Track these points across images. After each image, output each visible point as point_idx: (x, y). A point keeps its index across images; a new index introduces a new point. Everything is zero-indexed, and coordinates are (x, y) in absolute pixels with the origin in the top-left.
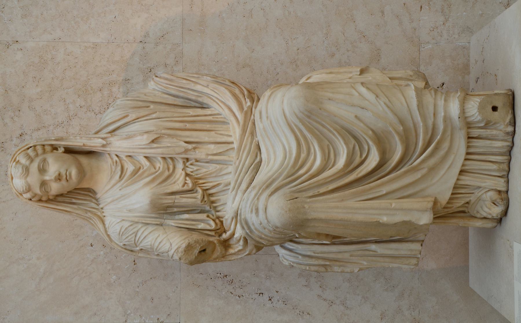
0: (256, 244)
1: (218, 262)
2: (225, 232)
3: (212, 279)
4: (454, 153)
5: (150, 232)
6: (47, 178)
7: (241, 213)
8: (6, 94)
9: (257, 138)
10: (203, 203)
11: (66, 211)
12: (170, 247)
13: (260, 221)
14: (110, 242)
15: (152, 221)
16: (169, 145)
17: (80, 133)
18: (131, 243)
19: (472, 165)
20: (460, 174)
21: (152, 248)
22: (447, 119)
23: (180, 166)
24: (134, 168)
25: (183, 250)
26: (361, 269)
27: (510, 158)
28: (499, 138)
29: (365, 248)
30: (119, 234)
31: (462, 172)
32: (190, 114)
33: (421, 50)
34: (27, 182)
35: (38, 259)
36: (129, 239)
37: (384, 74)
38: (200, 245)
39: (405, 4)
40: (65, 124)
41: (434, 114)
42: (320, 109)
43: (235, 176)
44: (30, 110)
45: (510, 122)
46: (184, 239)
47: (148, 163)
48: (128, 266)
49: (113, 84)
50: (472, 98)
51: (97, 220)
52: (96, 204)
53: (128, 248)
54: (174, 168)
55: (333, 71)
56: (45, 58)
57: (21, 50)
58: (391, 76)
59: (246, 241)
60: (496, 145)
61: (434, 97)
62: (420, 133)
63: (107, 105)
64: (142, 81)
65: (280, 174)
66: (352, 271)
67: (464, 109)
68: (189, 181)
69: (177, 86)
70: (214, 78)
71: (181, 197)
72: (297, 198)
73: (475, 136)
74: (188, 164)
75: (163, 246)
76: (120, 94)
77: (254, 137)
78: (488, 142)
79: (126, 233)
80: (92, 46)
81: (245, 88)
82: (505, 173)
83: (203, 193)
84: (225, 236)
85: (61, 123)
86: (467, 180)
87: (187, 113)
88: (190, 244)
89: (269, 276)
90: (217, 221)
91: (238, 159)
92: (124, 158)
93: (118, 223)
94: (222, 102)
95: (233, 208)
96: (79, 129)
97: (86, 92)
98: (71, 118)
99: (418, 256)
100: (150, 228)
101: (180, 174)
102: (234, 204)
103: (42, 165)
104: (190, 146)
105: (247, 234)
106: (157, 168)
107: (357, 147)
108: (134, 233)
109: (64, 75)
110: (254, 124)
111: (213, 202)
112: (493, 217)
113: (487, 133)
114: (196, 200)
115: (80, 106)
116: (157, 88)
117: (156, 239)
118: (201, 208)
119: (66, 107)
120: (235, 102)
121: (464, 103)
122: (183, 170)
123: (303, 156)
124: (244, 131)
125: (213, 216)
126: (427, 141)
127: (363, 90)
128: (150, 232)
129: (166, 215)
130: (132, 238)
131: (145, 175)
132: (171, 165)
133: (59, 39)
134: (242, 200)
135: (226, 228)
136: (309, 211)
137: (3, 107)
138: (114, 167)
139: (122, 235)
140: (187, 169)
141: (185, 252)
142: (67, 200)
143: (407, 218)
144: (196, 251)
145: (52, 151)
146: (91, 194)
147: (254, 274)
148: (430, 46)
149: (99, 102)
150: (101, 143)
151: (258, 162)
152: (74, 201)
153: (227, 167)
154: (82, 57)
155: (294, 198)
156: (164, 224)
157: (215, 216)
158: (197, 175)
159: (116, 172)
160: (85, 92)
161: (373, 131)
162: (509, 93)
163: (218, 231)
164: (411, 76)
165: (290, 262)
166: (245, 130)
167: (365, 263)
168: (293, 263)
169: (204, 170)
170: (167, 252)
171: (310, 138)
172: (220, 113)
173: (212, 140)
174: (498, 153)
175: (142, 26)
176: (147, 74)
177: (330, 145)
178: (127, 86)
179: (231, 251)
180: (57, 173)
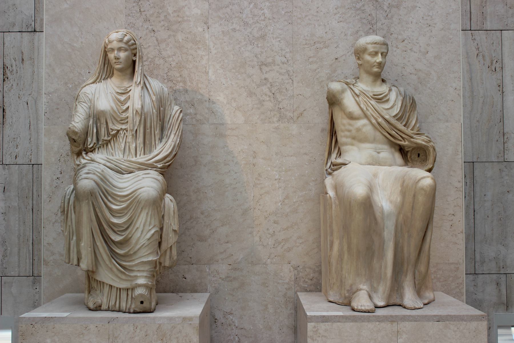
2: (86, 154)
6: (116, 52)
16: (135, 121)
19: (114, 291)
20: (110, 285)
22: (136, 277)
23: (124, 127)
24: (122, 100)
25: (74, 130)
30: (85, 93)
31: (111, 286)
32: (155, 132)
34: (113, 41)
35: (82, 42)
37: (174, 243)
39: (232, 255)
42: (142, 208)
45: (135, 311)
46: (80, 130)
51: (93, 80)
52: (105, 78)
54: (123, 124)
55: (176, 215)
56: (199, 44)
57: (204, 31)
58: (173, 247)
59: (78, 165)
61: (148, 270)
67: (141, 286)
68: (114, 132)
69: (174, 122)
71: (105, 128)
74: (125, 131)
80: (207, 71)
81: (172, 162)
84: (84, 153)
86: (106, 289)
89: (71, 177)
90: (93, 149)
92: (128, 94)
94: (163, 150)
95: (96, 158)
100: (87, 110)
101: (119, 127)
104: (134, 132)
106: (122, 114)
110: (146, 169)
111: (103, 146)
117: (81, 114)
120: (161, 158)
121: (144, 286)
122: (121, 128)
123: (119, 199)
125: (96, 146)
131: (118, 107)
138: (123, 88)
140: (122, 131)
144: (74, 137)
145: (132, 53)
146: (111, 75)
148: (207, 270)
150: (137, 81)
151: (122, 172)
152: (106, 66)
153: (122, 154)
157: (95, 147)
158: (118, 137)
161: (131, 237)
162: (151, 309)
164: (173, 258)
166: (142, 165)
167: (66, 234)
168: (66, 193)
169: (121, 141)
178: (183, 91)
179: (75, 157)
180: (119, 57)
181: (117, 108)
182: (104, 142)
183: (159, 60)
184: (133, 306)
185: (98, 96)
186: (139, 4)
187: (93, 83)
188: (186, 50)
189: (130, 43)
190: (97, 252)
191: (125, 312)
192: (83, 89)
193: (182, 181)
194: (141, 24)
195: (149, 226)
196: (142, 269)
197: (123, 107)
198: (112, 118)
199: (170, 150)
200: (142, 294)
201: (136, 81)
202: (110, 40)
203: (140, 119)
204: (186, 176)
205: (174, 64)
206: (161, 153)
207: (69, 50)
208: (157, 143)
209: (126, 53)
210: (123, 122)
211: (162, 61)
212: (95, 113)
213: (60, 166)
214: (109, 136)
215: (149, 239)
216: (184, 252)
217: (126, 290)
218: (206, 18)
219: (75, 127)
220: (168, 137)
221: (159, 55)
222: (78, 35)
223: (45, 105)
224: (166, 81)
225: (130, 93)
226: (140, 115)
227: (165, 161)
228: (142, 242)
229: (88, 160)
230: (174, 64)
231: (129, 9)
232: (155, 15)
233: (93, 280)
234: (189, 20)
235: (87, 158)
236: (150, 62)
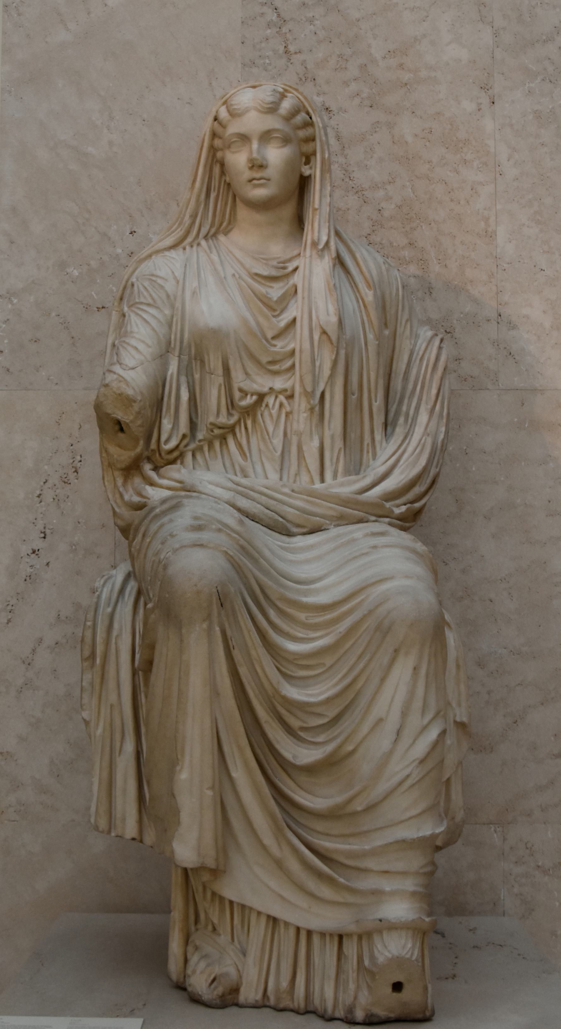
0: (133, 526)
1: (101, 457)
2: (156, 469)
3: (72, 445)
5: (153, 329)
7: (191, 497)
9: (332, 526)
10: (208, 426)
11: (194, 181)
13: (176, 535)
14: (138, 260)
15: (176, 334)
16: (317, 364)
18: (137, 296)
20: (269, 917)
21: (126, 334)
23: (279, 383)
24: (275, 299)
26: (87, 723)
27: (302, 1012)
28: (341, 994)
29: (126, 732)
31: (274, 921)
33: (491, 826)
38: (132, 422)
40: (349, 183)
41: (386, 872)
44: (373, 124)
45: (372, 1015)
47: (282, 324)
48: (95, 297)
50: (418, 944)
53: (128, 291)
54: (276, 373)
57: (479, 110)
59: (140, 507)
60: (326, 987)
62: (349, 844)
63: (385, 255)
65: (266, 573)
66: (84, 707)
67: (396, 929)
68: (249, 400)
69: (424, 377)
70: (442, 446)
71: (220, 385)
72: (222, 606)
73: (345, 950)
74: (282, 398)
75: (130, 354)
78: (332, 972)
79: (154, 287)
82: (272, 1002)
84: (147, 468)
85: (350, 177)
87: (376, 397)
88: (133, 404)
89: (76, 549)
90: (176, 454)
91: (293, 491)
92: (291, 282)
93: (173, 272)
94: (398, 461)
95: (201, 483)
98: (360, 193)
99: (113, 830)
102: (207, 484)
105: (153, 509)
106: (274, 342)
109: (436, 182)
110: (361, 521)
111: (211, 445)
112: (189, 976)
113: (351, 972)
114: (216, 413)
115: (381, 209)
116: (419, 342)
118: (199, 423)
119: (380, 186)
120: (400, 485)
122: (271, 389)
123: (302, 616)
124: (345, 502)
125: (186, 446)
126: (335, 856)
127: (433, 734)
128: (153, 329)
130: (145, 297)
131: (262, 320)
132: (280, 366)
133: (501, 173)
134: (216, 500)
135: (162, 471)
136: (197, 629)
137: (378, 79)
138: (275, 263)
139: (151, 279)
141: (119, 394)
142: (215, 182)
143: (185, 816)
144: (120, 415)
145: (302, 154)
146: (225, 224)
147: (79, 522)
149: (390, 241)
150: (319, 239)
152: (213, 195)
154: (469, 212)
155: (222, 600)
156: (171, 356)
157: (185, 449)
158: (262, 415)
160: (406, 217)
163: (157, 455)
165: (99, 590)
168: (99, 597)
169: (271, 428)
170: (118, 361)
171: (338, 631)
172: (377, 457)
174: (312, 990)
175: (528, 318)
176: (442, 326)
177: (324, 669)
179: (120, 481)
181: (258, 324)
183: (346, 198)
184: (364, 998)
185: (195, 284)
186: (284, 30)
187: (173, 247)
190: (230, 801)
191: (332, 1019)
192: (143, 265)
196: (399, 866)
198: (243, 353)
199: (423, 462)
201: (316, 238)
202: (235, 107)
203: (334, 357)
205: (389, 209)
206: (397, 471)
210: (276, 367)
212: (185, 341)
213: (42, 516)
217: (336, 939)
218: (486, 74)
219: (127, 383)
220: (410, 421)
225: (297, 279)
226: (335, 344)
227: (410, 495)
229: (169, 488)
230: (389, 209)
233: (209, 894)
234: (435, 77)
235: (165, 482)
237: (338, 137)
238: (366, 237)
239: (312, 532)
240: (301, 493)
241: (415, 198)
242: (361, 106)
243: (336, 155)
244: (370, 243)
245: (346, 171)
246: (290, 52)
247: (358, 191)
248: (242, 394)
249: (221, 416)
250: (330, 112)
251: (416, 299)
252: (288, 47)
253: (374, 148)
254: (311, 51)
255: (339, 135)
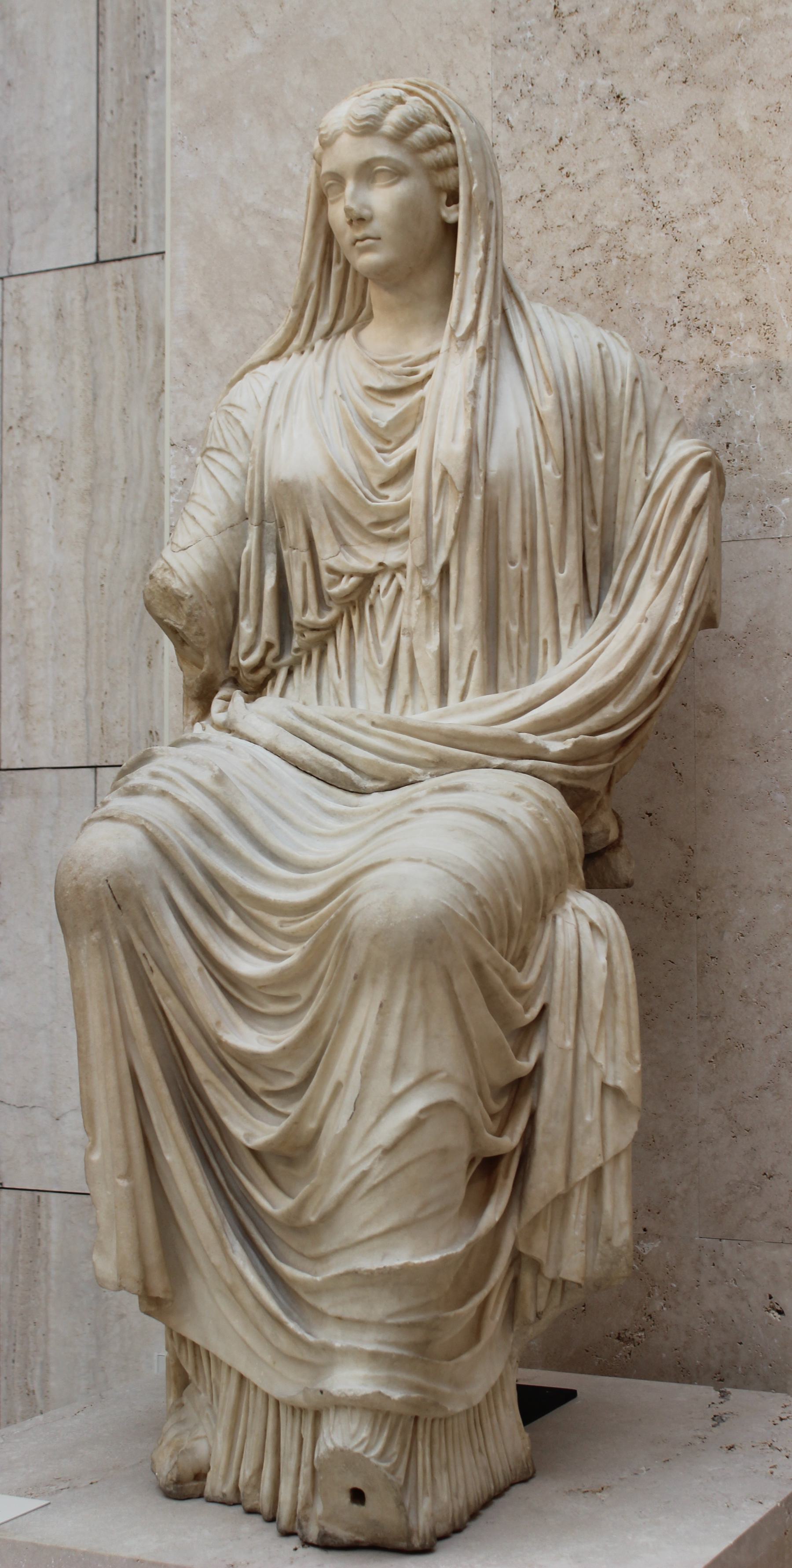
4: (274, 1363)
8: (731, 38)
9: (429, 777)
12: (179, 547)
15: (252, 492)
16: (436, 520)
17: (628, 257)
23: (392, 556)
24: (383, 424)
30: (230, 405)
34: (336, 135)
36: (215, 433)
37: (617, 1157)
40: (651, 212)
43: (330, 718)
44: (688, 110)
46: (194, 585)
49: (767, 336)
54: (390, 540)
61: (390, 1321)
63: (708, 324)
64: (777, 418)
67: (346, 1407)
68: (346, 584)
71: (304, 566)
76: (739, 356)
77: (434, 768)
79: (229, 422)
83: (322, 627)
85: (653, 202)
88: (182, 602)
90: (263, 672)
91: (373, 724)
92: (419, 394)
93: (256, 398)
96: (638, 253)
97: (743, 260)
98: (668, 227)
103: (385, 167)
106: (384, 492)
107: (289, 1083)
108: (226, 444)
117: (205, 507)
119: (699, 210)
120: (566, 706)
121: (365, 1409)
122: (381, 564)
123: (274, 921)
124: (453, 739)
125: (277, 659)
126: (296, 1288)
128: (222, 488)
129: (275, 528)
130: (216, 439)
136: (85, 942)
137: (695, 35)
138: (398, 367)
141: (164, 589)
145: (439, 190)
149: (715, 299)
151: (353, 784)
155: (119, 899)
159: (381, 377)
160: (741, 256)
164: (609, 1240)
166: (457, 742)
173: (453, 644)
178: (760, 375)
180: (365, 213)
181: (359, 467)
182: (306, 635)
183: (648, 237)
187: (275, 356)
188: (773, 167)
189: (418, 136)
193: (762, 824)
194: (561, 75)
195: (395, 1075)
196: (355, 1311)
197: (385, 460)
198: (336, 514)
199: (621, 667)
200: (349, 1451)
204: (780, 797)
205: (714, 245)
207: (265, 241)
208: (565, 629)
209: (401, 189)
210: (387, 531)
211: (658, 239)
214: (331, 604)
215: (389, 1151)
216: (770, 1177)
220: (623, 599)
221: (643, 214)
222: (296, 170)
223: (171, 493)
224: (678, 333)
227: (593, 721)
228: (353, 1167)
230: (714, 245)
231: (510, 14)
232: (626, 19)
236: (606, 249)
237: (636, 140)
238: (678, 298)
239: (395, 786)
240: (383, 727)
241: (755, 223)
242: (669, 84)
243: (632, 169)
244: (686, 307)
245: (647, 193)
246: (562, 13)
247: (666, 223)
248: (332, 576)
249: (309, 611)
250: (623, 101)
251: (756, 390)
252: (559, 7)
253: (690, 150)
254: (593, 6)
255: (636, 136)
